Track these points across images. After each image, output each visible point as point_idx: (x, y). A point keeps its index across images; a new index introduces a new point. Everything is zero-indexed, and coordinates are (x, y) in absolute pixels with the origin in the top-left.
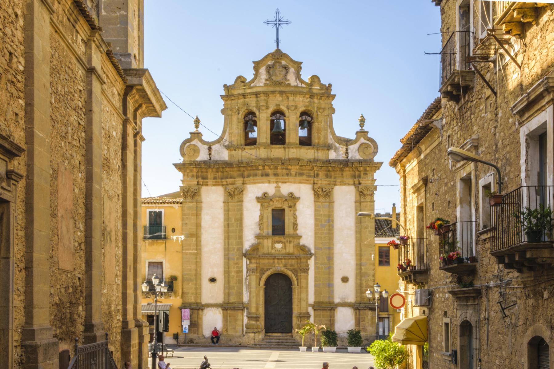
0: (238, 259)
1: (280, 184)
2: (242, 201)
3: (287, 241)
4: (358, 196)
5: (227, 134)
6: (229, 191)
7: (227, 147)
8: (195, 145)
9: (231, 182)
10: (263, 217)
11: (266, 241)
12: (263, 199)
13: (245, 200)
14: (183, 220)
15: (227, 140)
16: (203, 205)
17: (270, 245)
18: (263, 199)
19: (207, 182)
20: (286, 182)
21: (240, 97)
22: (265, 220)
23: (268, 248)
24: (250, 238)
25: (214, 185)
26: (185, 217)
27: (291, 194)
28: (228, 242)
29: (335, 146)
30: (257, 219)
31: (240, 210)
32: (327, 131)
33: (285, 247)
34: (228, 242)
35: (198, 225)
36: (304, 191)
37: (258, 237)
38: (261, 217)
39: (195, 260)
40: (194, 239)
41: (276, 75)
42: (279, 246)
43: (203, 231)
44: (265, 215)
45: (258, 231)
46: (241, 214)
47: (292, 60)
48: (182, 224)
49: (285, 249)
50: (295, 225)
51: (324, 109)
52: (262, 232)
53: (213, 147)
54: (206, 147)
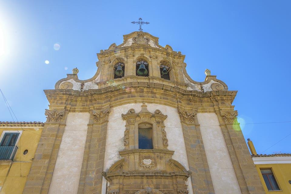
0: (96, 183)
1: (146, 104)
2: (108, 121)
3: (158, 156)
4: (221, 120)
5: (99, 76)
6: (95, 114)
7: (97, 84)
8: (69, 83)
9: (98, 108)
10: (128, 132)
11: (132, 156)
12: (129, 116)
13: (109, 121)
14: (40, 140)
15: (98, 79)
16: (66, 128)
17: (137, 160)
18: (129, 116)
19: (75, 108)
20: (152, 103)
21: (112, 53)
22: (131, 135)
23: (135, 165)
24: (113, 155)
25: (81, 111)
26: (43, 138)
27: (158, 112)
28: (87, 165)
29: (191, 85)
30: (122, 135)
31: (105, 130)
32: (183, 75)
33: (155, 163)
34: (87, 165)
35: (56, 147)
36: (170, 113)
37: (121, 153)
38: (127, 133)
39: (40, 187)
40: (47, 161)
41: (140, 41)
42: (148, 162)
43: (60, 154)
44: (131, 130)
45: (123, 148)
46: (105, 133)
47: (151, 36)
48: (38, 145)
49: (156, 165)
50: (165, 141)
51: (178, 63)
52: (127, 147)
53: (86, 84)
54: (79, 84)
